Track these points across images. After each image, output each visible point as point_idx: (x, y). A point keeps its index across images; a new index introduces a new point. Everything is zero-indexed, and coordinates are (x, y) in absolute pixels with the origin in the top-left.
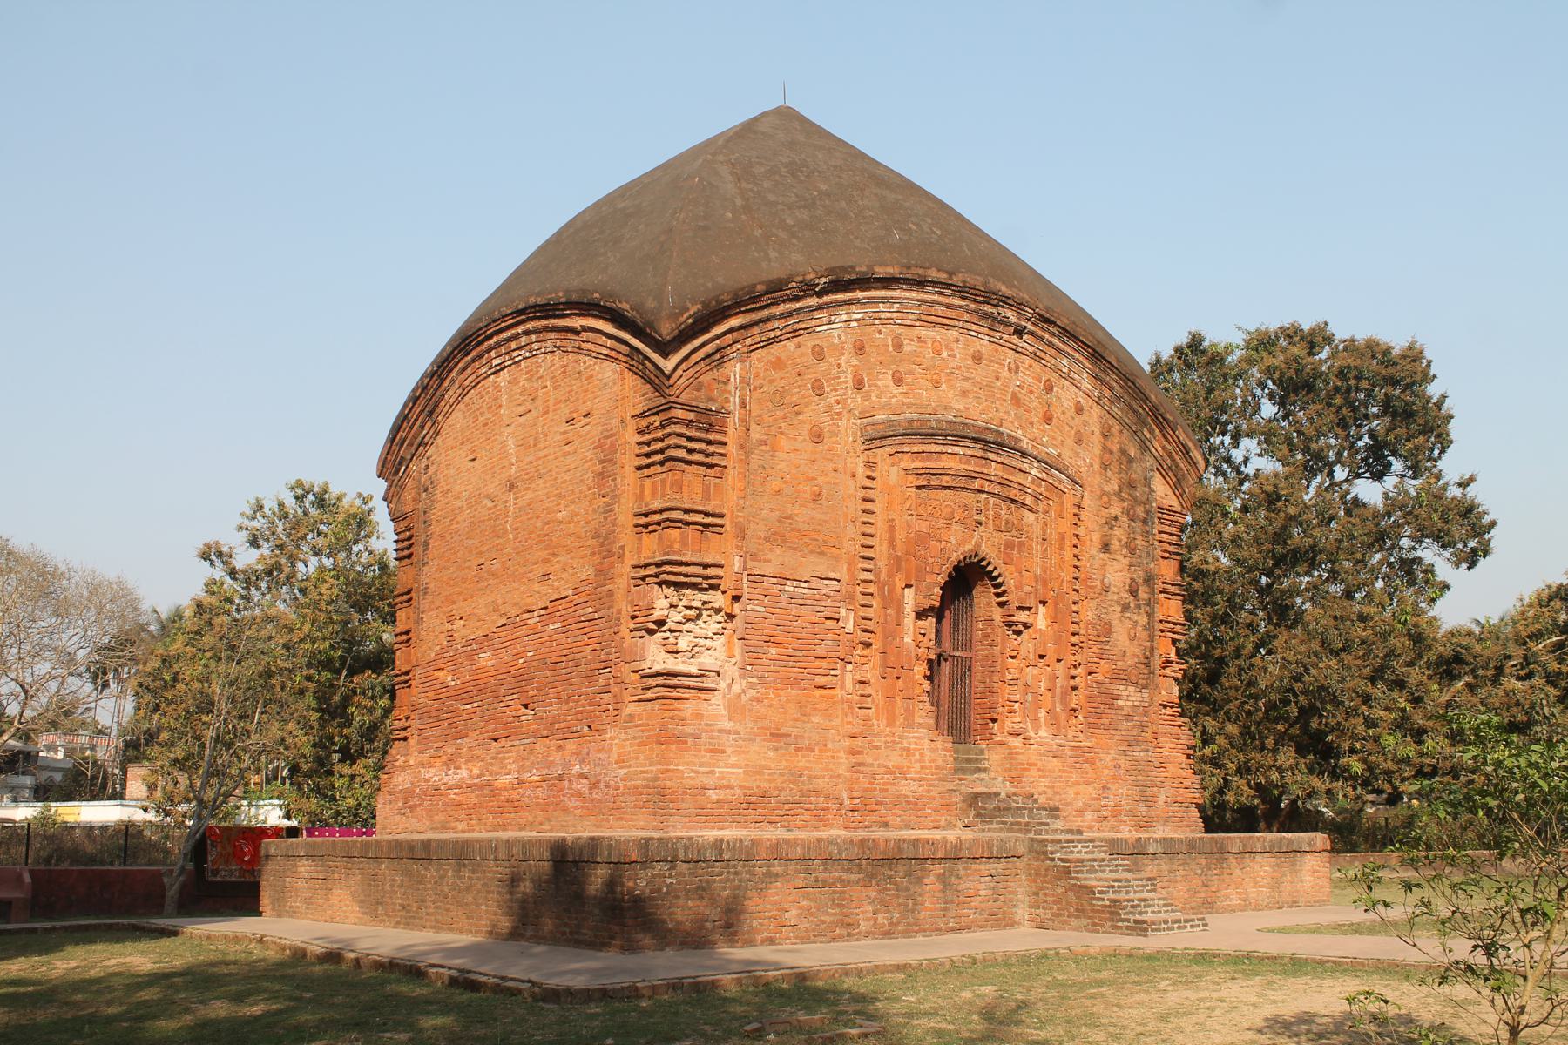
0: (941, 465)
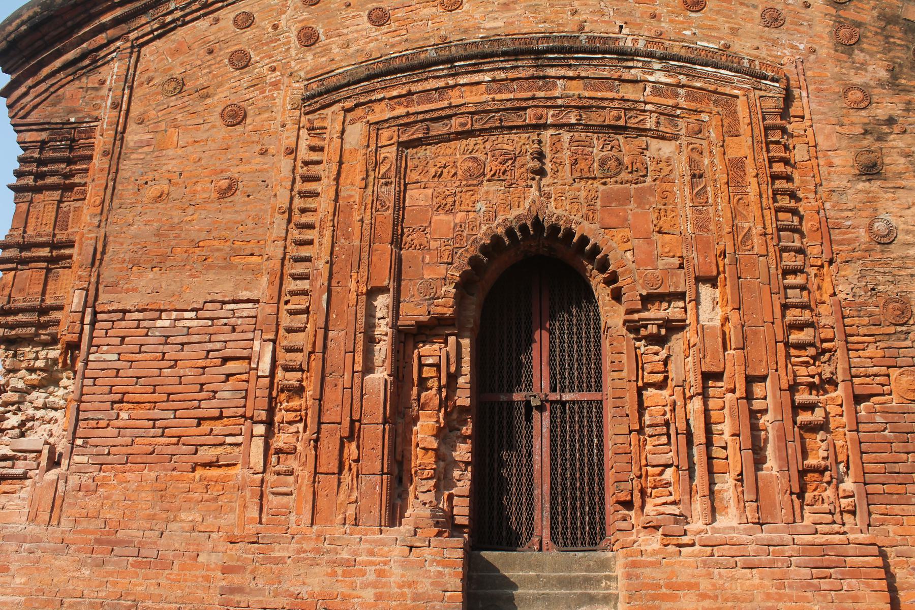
0: (445, 103)
